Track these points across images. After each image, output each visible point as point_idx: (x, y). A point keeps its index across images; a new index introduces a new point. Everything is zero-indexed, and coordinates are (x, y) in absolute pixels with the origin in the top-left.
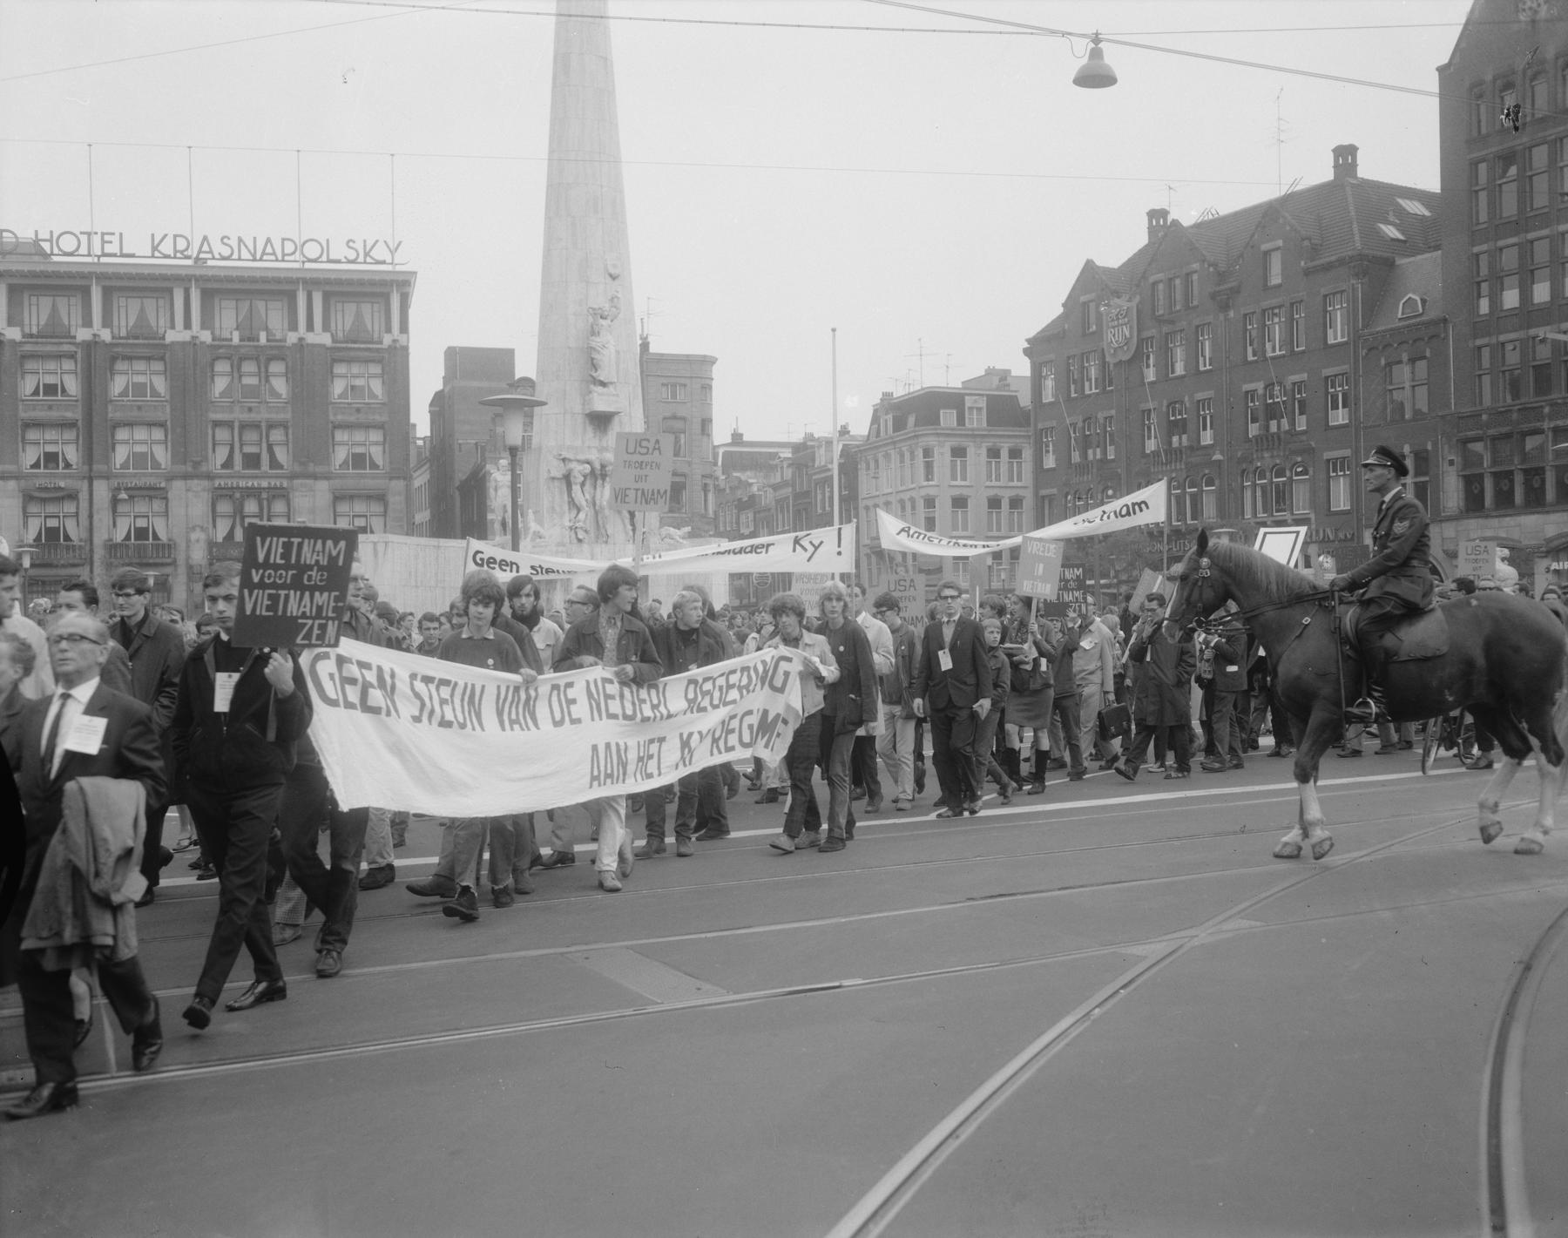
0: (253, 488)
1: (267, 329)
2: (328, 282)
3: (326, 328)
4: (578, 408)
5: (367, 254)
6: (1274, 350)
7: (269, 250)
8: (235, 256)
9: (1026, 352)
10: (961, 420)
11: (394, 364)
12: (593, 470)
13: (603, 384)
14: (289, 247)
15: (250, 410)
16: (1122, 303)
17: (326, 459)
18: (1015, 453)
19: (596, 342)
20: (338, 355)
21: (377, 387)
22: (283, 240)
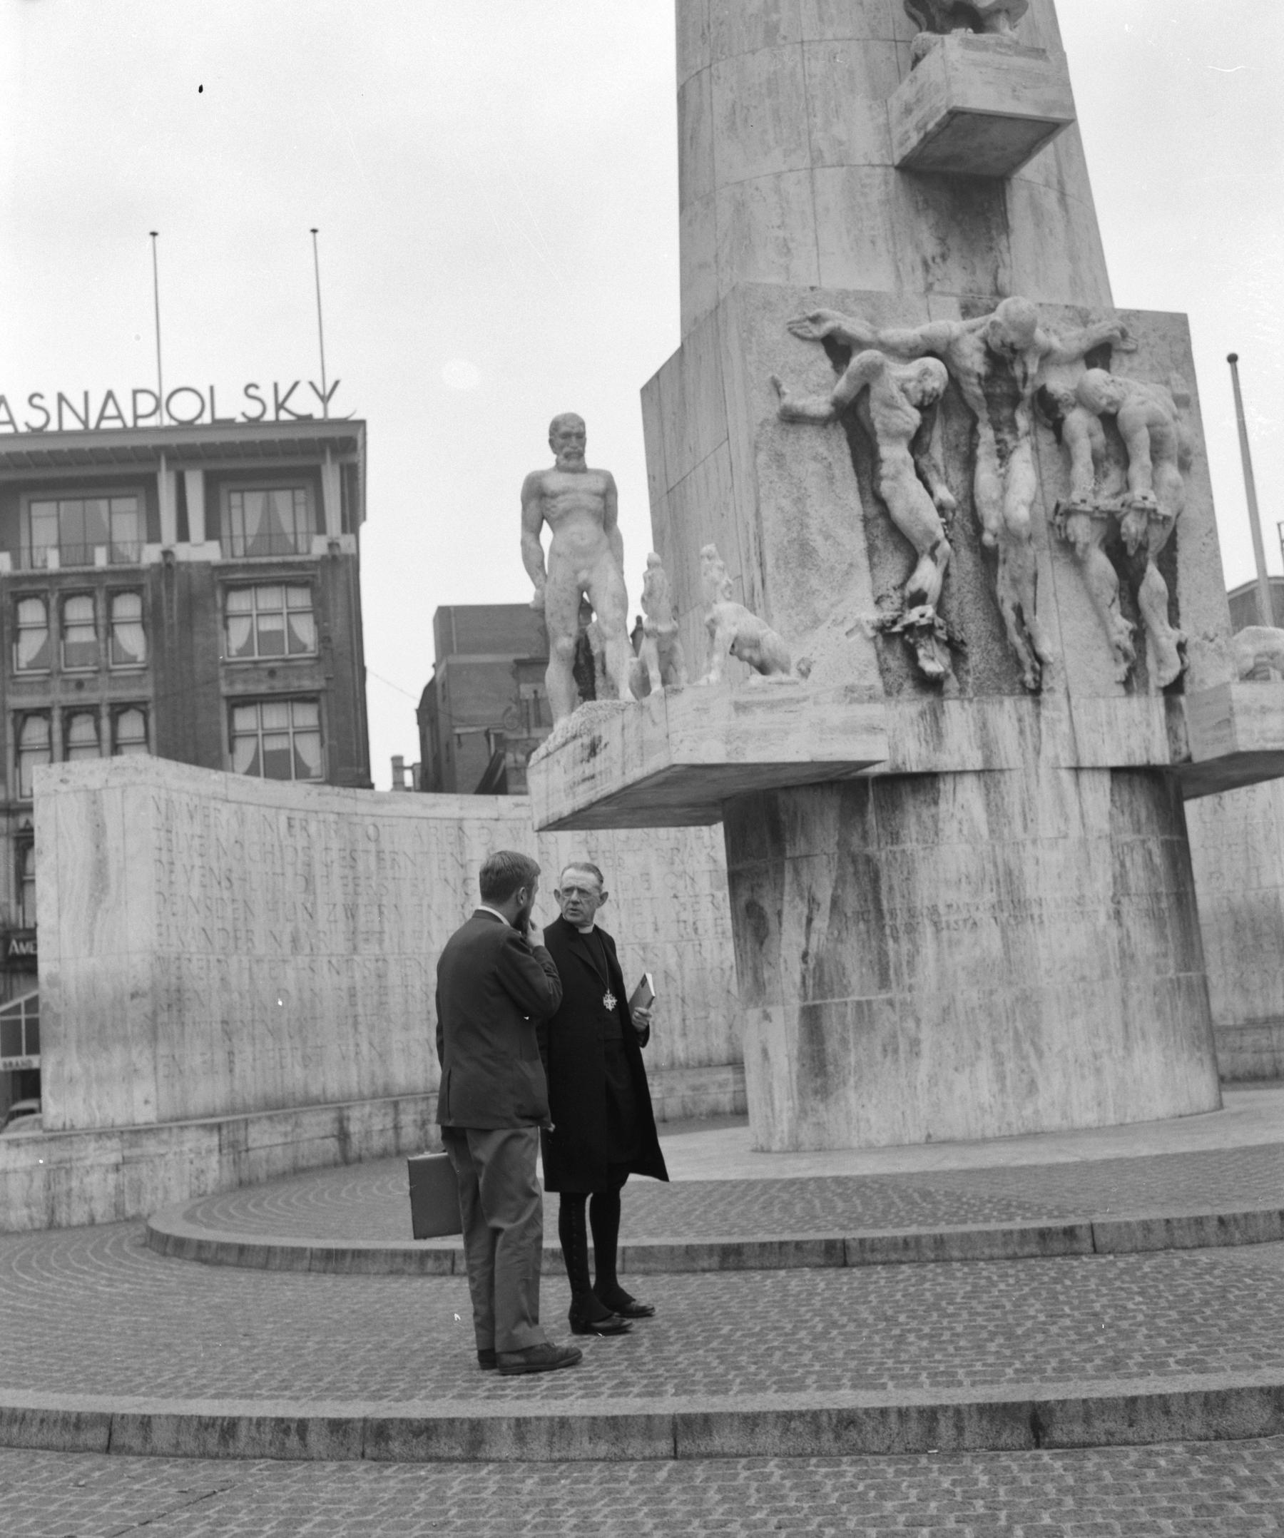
1: (110, 545)
3: (212, 533)
5: (279, 406)
7: (111, 410)
11: (332, 586)
12: (954, 381)
15: (80, 685)
20: (229, 579)
21: (306, 631)
22: (135, 392)
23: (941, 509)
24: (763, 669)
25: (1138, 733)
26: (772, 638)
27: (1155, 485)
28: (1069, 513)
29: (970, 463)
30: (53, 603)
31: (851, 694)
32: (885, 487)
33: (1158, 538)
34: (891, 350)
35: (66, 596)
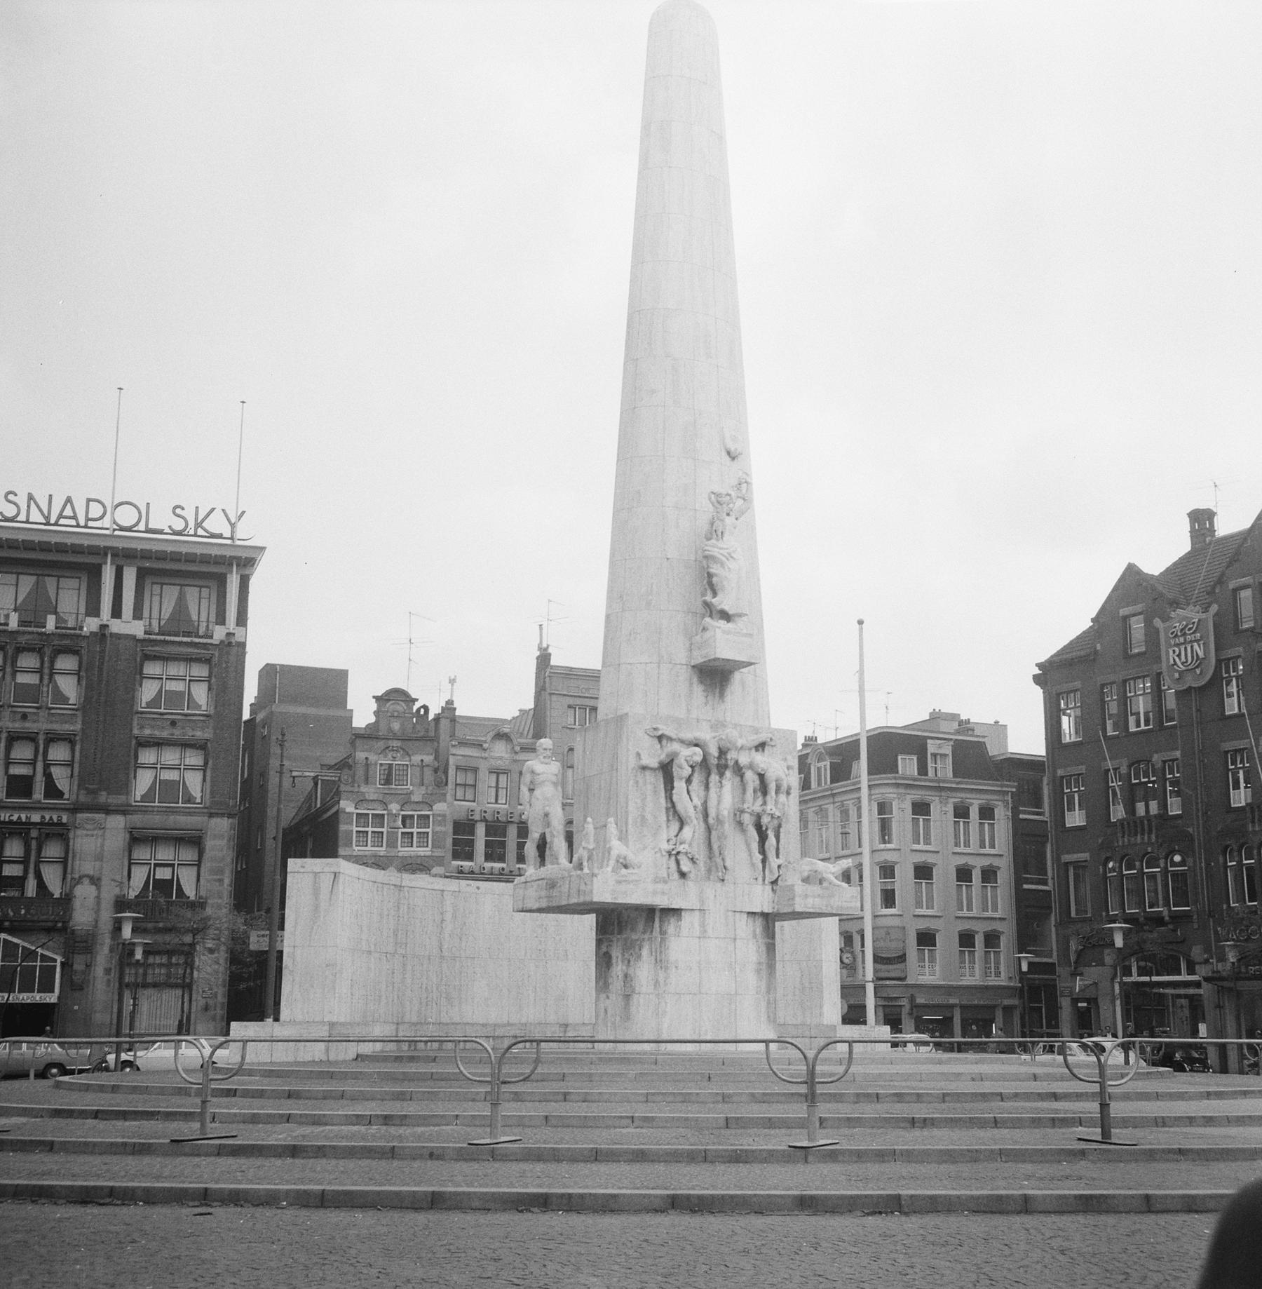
0: (19, 822)
2: (146, 555)
3: (138, 615)
4: (681, 656)
5: (198, 525)
6: (1138, 725)
8: (22, 517)
9: (1037, 680)
10: (923, 770)
12: (705, 759)
13: (725, 616)
14: (96, 510)
15: (24, 717)
16: (1193, 614)
17: (125, 787)
18: (987, 813)
19: (715, 548)
20: (149, 650)
21: (200, 694)
22: (89, 500)
23: (695, 807)
24: (626, 867)
25: (762, 900)
26: (631, 857)
27: (776, 802)
28: (742, 811)
29: (707, 787)
30: (10, 654)
31: (657, 880)
32: (675, 798)
33: (776, 822)
34: (682, 742)
35: (19, 650)
